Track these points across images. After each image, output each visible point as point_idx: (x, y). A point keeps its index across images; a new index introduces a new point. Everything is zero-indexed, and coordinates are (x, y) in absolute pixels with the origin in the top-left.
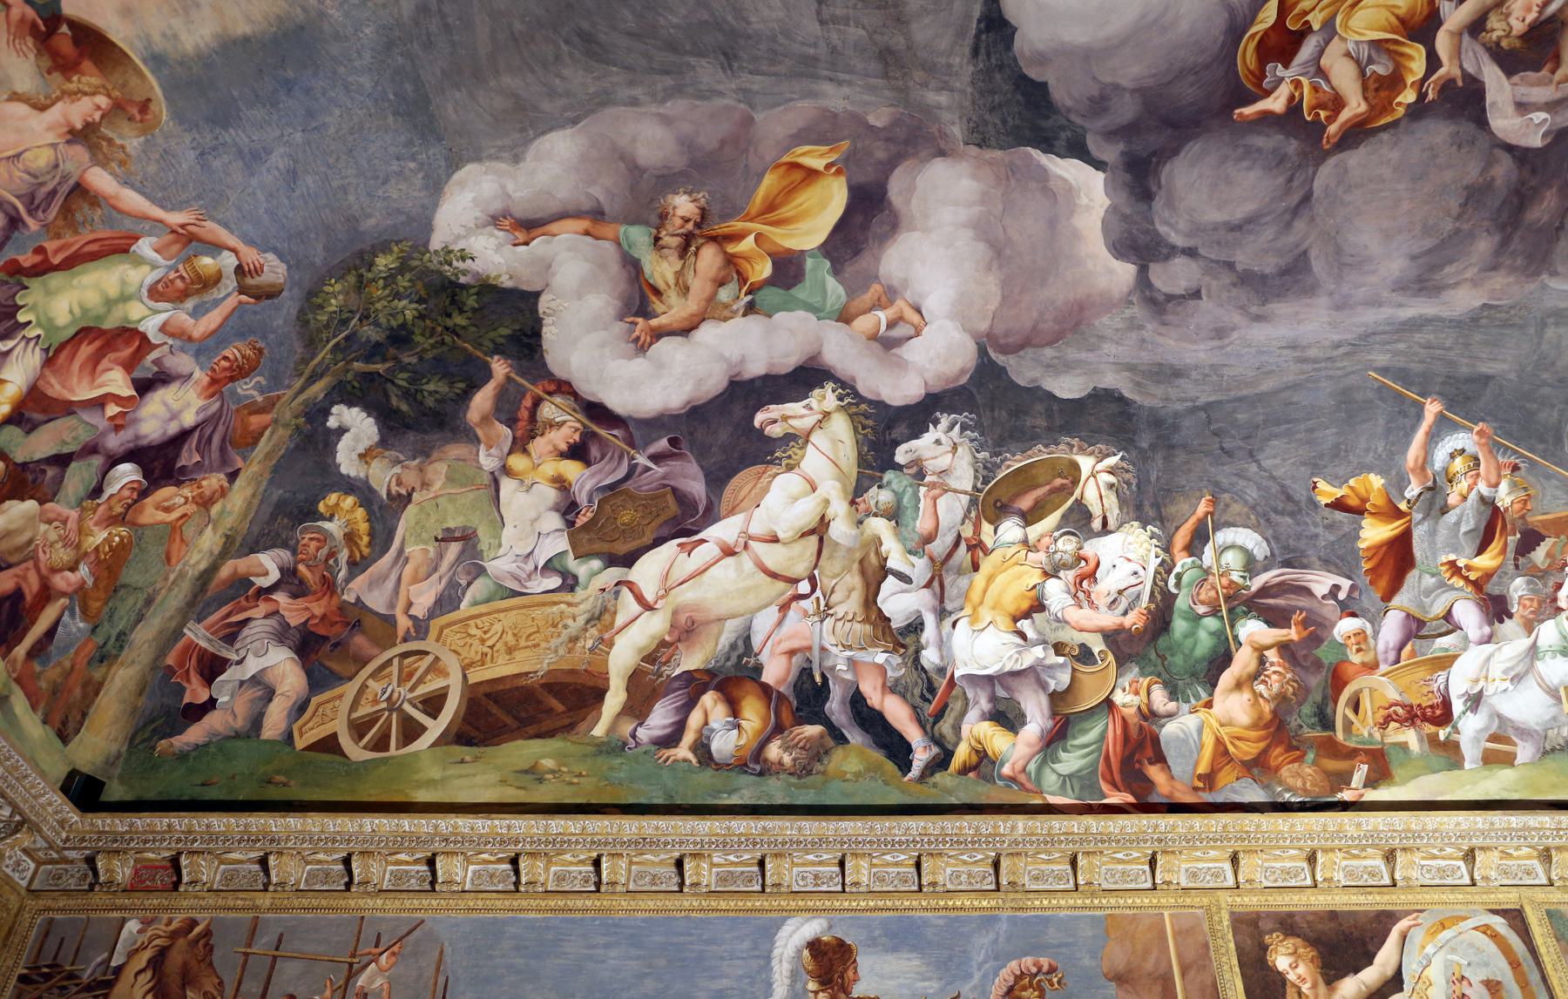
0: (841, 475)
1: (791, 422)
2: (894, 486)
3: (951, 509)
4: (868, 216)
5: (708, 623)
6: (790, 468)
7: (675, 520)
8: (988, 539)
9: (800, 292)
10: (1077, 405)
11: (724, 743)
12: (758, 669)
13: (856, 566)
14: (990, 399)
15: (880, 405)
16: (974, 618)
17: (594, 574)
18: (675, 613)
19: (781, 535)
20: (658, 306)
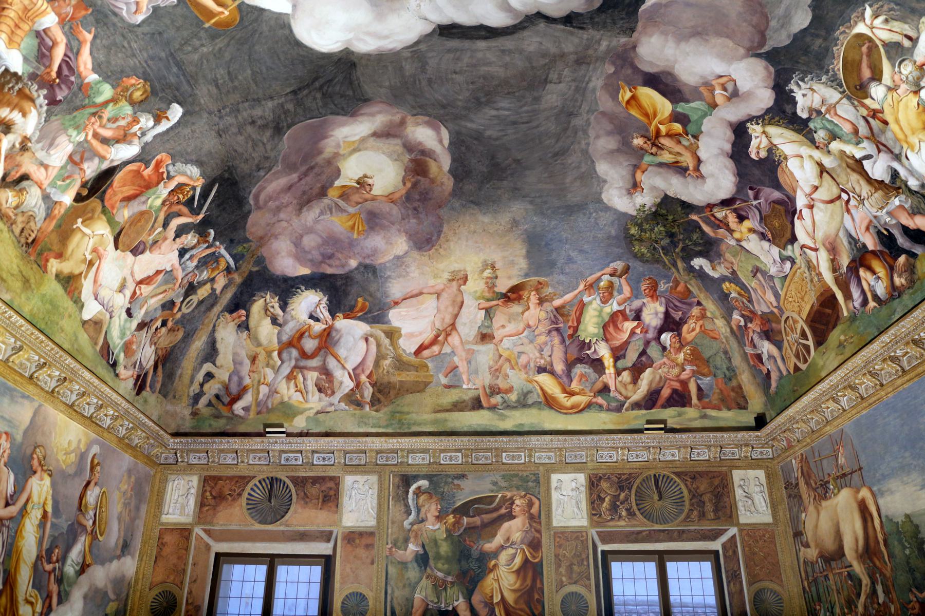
0: (801, 143)
1: (762, 146)
2: (818, 127)
3: (847, 111)
4: (662, 82)
5: (835, 240)
6: (786, 158)
7: (787, 211)
8: (875, 106)
9: (694, 117)
10: (817, 20)
11: (881, 289)
12: (864, 246)
13: (849, 170)
14: (788, 62)
15: (768, 111)
16: (912, 147)
17: (793, 251)
18: (824, 245)
19: (816, 184)
20: (684, 164)
